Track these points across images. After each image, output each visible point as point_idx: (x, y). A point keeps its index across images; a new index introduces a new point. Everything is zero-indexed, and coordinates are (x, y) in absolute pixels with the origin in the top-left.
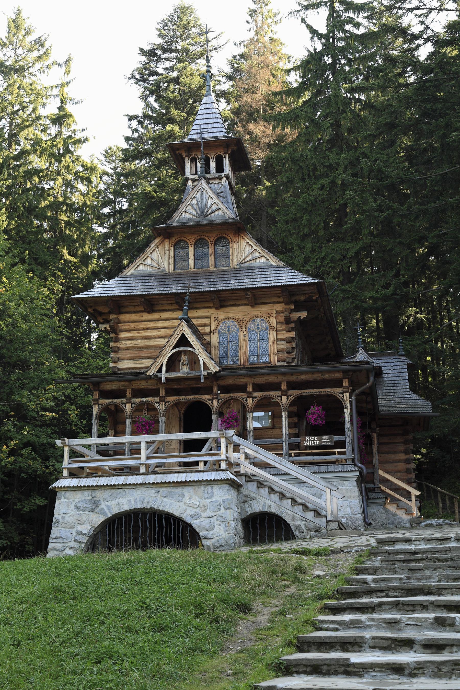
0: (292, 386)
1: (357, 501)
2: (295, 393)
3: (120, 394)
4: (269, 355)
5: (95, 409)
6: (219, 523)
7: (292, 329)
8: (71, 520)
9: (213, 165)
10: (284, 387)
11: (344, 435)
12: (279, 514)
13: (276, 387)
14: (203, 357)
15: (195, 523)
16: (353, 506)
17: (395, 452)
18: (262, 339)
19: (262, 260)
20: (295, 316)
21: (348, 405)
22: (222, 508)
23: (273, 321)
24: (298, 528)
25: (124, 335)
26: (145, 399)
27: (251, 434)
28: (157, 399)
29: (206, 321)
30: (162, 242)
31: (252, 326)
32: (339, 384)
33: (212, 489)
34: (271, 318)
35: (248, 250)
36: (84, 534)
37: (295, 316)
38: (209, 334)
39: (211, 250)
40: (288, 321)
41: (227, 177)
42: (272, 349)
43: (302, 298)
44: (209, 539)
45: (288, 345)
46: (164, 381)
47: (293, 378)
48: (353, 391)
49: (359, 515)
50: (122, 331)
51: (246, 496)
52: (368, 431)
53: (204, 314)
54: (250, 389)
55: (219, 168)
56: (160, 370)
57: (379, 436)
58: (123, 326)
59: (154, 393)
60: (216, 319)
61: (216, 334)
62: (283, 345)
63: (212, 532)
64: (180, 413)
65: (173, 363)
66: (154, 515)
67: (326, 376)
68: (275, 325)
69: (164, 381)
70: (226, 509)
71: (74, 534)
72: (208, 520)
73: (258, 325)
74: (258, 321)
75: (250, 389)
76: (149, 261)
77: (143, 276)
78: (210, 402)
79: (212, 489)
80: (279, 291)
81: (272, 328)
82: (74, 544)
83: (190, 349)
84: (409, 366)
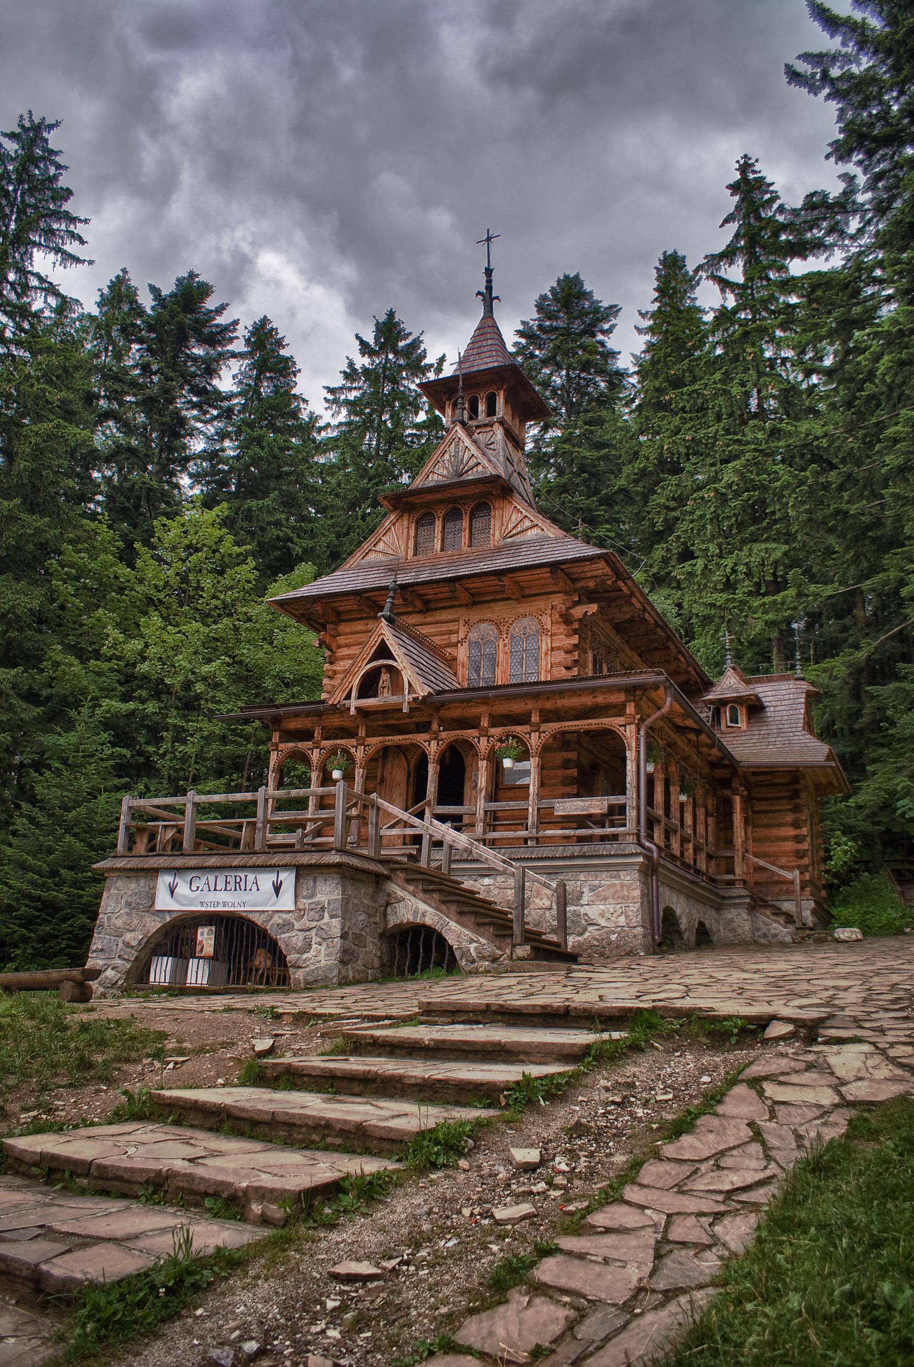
0: (548, 716)
1: (637, 905)
2: (552, 727)
3: (306, 735)
4: (539, 673)
5: (274, 758)
6: (319, 939)
7: (575, 632)
8: (119, 922)
9: (482, 407)
10: (535, 718)
11: (624, 793)
12: (438, 927)
13: (522, 719)
14: (408, 674)
15: (282, 938)
16: (630, 913)
17: (780, 825)
18: (533, 649)
19: (535, 531)
20: (578, 612)
21: (634, 745)
22: (326, 915)
23: (547, 620)
24: (465, 953)
25: (344, 652)
26: (338, 742)
27: (483, 793)
28: (354, 741)
29: (452, 627)
30: (401, 517)
31: (516, 629)
32: (619, 710)
33: (315, 882)
34: (544, 617)
35: (516, 517)
36: (132, 947)
37: (578, 612)
38: (455, 645)
39: (465, 523)
40: (566, 619)
41: (502, 423)
42: (544, 663)
43: (591, 584)
44: (299, 967)
45: (568, 656)
46: (353, 712)
47: (549, 705)
48: (642, 720)
49: (640, 929)
50: (339, 647)
51: (389, 895)
52: (728, 792)
53: (450, 617)
54: (485, 723)
55: (491, 411)
56: (348, 697)
57: (748, 801)
58: (342, 640)
59: (350, 733)
60: (466, 623)
61: (466, 645)
62: (560, 656)
63: (305, 956)
64: (408, 763)
65: (368, 687)
66: (233, 921)
67: (600, 699)
68: (549, 627)
69: (353, 712)
70: (332, 917)
71: (121, 945)
72: (301, 935)
73: (525, 628)
74: (526, 621)
75: (485, 723)
76: (381, 546)
77: (372, 566)
78: (426, 744)
79: (315, 882)
80: (545, 573)
81: (544, 631)
82: (119, 962)
83: (390, 662)
84: (809, 695)
